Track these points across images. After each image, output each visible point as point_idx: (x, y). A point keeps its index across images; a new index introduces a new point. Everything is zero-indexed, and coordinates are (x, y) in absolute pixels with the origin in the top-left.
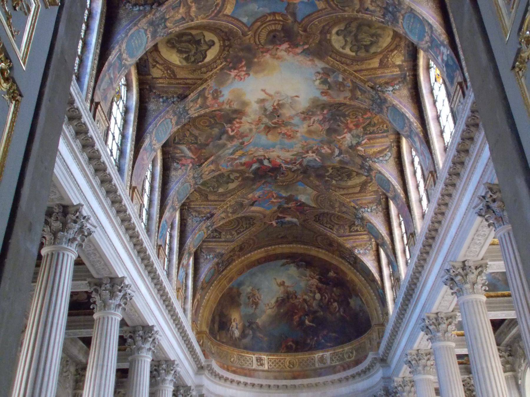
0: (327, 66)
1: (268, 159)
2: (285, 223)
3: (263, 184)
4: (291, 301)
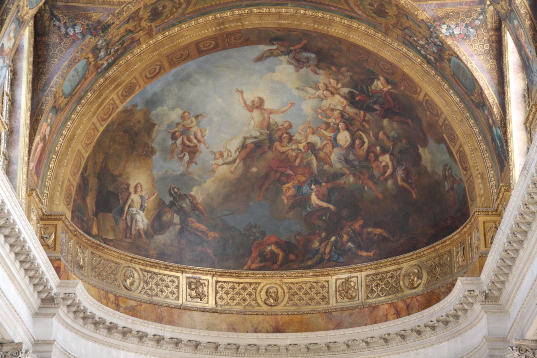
4: (277, 144)
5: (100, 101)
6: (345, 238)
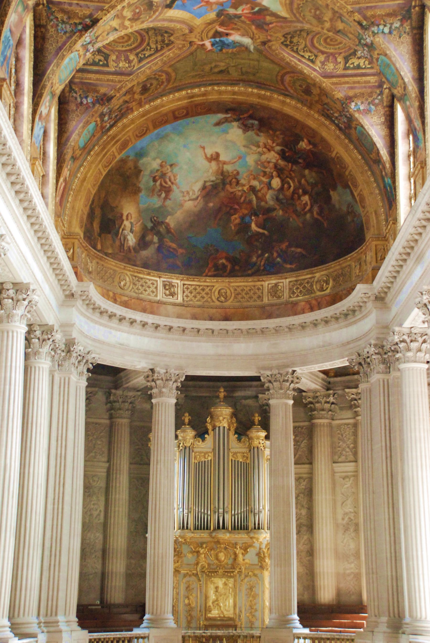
4: (228, 187)
5: (104, 153)
6: (275, 255)
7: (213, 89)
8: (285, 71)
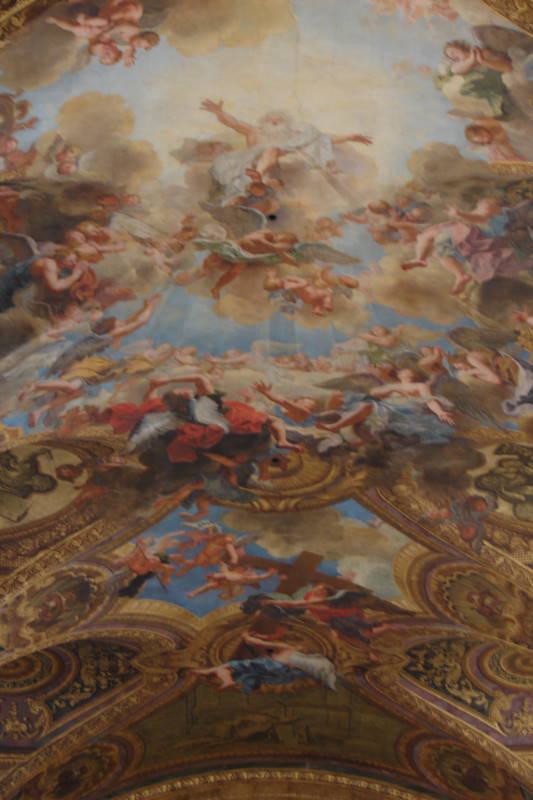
0: (501, 21)
1: (216, 397)
2: (273, 675)
3: (186, 503)
7: (239, 779)
8: (418, 732)
